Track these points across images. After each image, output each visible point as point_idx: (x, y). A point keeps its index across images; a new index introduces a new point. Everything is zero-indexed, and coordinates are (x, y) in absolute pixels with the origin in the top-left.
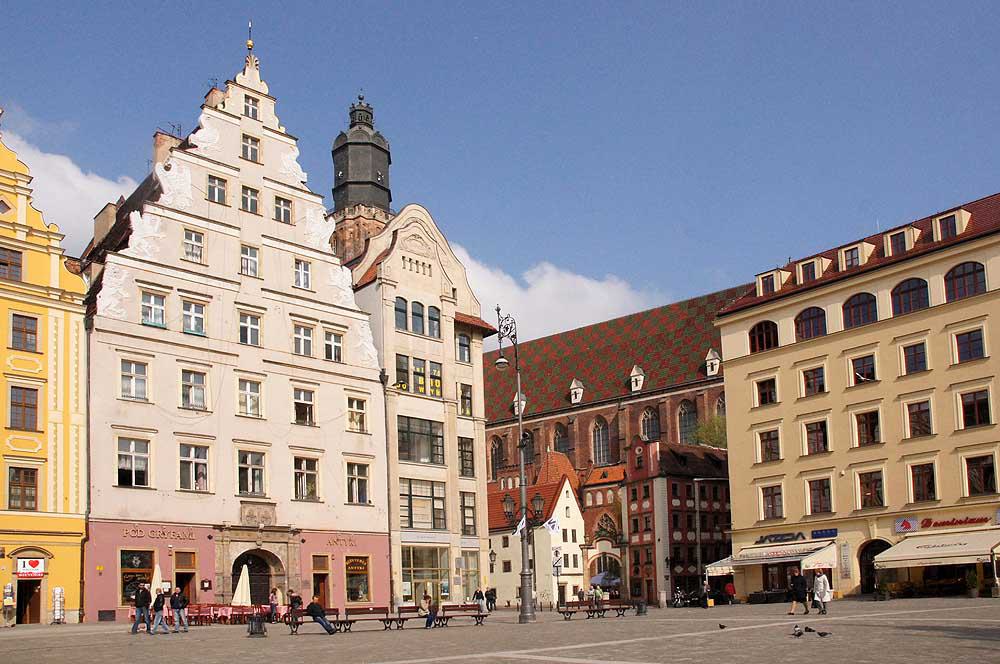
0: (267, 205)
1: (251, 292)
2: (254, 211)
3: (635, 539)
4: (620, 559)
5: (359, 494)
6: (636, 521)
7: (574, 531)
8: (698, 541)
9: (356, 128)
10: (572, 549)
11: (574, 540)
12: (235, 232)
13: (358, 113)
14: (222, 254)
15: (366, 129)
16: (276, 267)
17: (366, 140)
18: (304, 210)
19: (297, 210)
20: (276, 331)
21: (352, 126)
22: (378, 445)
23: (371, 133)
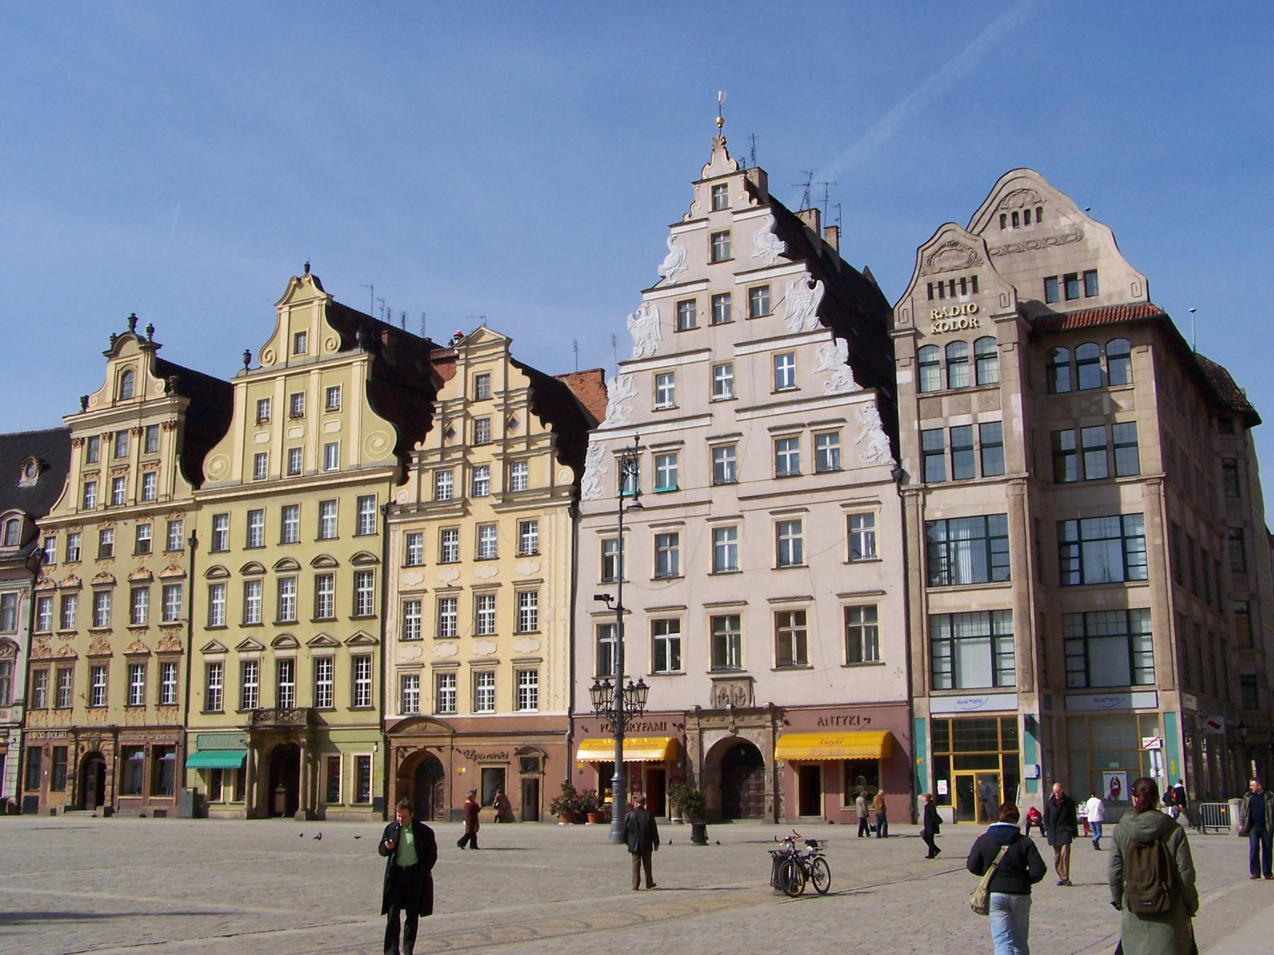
0: (739, 303)
1: (725, 420)
5: (859, 648)
14: (692, 388)
20: (755, 460)
22: (886, 576)
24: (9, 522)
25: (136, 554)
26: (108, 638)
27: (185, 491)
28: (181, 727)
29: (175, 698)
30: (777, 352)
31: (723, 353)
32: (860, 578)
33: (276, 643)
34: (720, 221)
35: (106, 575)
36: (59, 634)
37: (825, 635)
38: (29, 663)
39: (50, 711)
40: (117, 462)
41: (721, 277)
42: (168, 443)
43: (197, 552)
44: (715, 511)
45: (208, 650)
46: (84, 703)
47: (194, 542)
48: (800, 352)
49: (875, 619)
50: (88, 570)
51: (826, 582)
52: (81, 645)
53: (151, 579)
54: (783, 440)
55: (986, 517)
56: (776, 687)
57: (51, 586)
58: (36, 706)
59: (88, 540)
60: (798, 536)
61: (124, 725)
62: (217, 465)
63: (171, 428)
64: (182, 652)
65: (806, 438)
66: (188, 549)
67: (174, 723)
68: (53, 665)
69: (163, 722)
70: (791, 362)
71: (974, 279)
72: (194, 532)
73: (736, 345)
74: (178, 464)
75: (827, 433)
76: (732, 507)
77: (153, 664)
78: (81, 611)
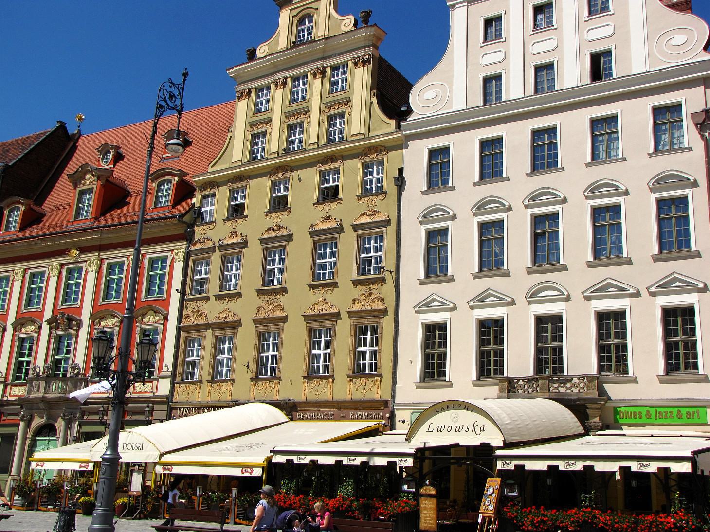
24: (160, 185)
25: (319, 203)
26: (282, 299)
27: (384, 127)
28: (385, 403)
29: (374, 367)
33: (533, 296)
35: (280, 227)
36: (218, 297)
38: (179, 330)
39: (205, 384)
40: (294, 107)
42: (360, 80)
43: (404, 195)
45: (425, 306)
46: (251, 375)
47: (400, 180)
50: (257, 224)
52: (247, 308)
53: (340, 229)
57: (209, 244)
58: (189, 379)
59: (257, 195)
61: (303, 398)
62: (429, 94)
63: (364, 63)
64: (384, 312)
66: (392, 189)
67: (376, 397)
68: (209, 333)
69: (358, 396)
72: (401, 171)
74: (374, 100)
77: (344, 329)
78: (249, 271)
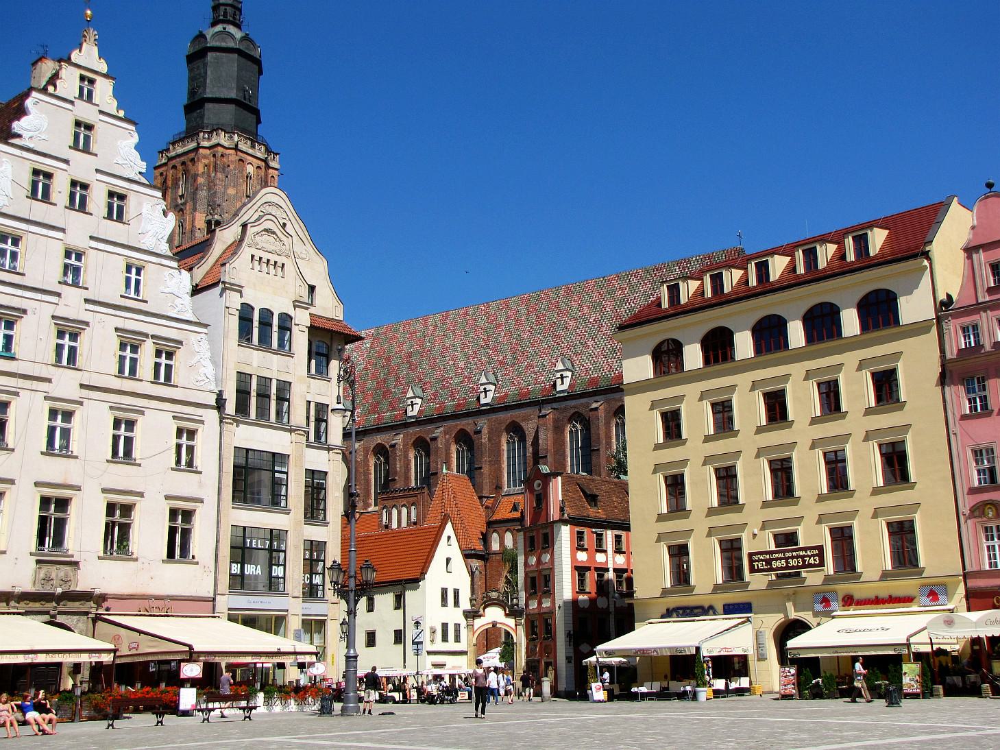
0: (98, 200)
1: (72, 304)
2: (83, 208)
3: (534, 605)
4: (516, 631)
6: (533, 579)
7: (456, 592)
8: (612, 609)
9: (219, 28)
10: (454, 616)
11: (456, 604)
12: (59, 235)
13: (222, 8)
15: (231, 29)
16: (104, 275)
17: (231, 44)
18: (140, 204)
19: (131, 206)
21: (214, 24)
23: (238, 34)
30: (130, 260)
31: (78, 240)
32: (185, 484)
34: (85, 112)
37: (149, 531)
41: (82, 166)
44: (55, 390)
48: (149, 267)
49: (129, 516)
51: (154, 483)
54: (130, 342)
55: (247, 450)
56: (98, 574)
60: (129, 434)
65: (148, 348)
70: (138, 273)
71: (283, 265)
73: (91, 238)
75: (166, 350)
76: (76, 394)
